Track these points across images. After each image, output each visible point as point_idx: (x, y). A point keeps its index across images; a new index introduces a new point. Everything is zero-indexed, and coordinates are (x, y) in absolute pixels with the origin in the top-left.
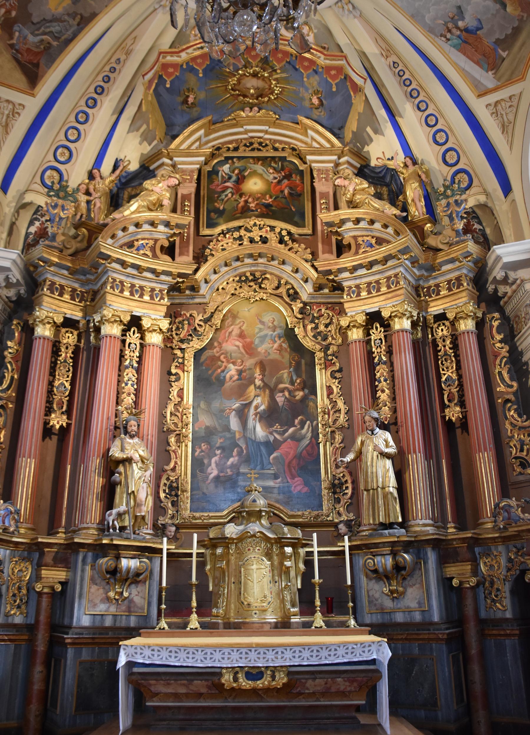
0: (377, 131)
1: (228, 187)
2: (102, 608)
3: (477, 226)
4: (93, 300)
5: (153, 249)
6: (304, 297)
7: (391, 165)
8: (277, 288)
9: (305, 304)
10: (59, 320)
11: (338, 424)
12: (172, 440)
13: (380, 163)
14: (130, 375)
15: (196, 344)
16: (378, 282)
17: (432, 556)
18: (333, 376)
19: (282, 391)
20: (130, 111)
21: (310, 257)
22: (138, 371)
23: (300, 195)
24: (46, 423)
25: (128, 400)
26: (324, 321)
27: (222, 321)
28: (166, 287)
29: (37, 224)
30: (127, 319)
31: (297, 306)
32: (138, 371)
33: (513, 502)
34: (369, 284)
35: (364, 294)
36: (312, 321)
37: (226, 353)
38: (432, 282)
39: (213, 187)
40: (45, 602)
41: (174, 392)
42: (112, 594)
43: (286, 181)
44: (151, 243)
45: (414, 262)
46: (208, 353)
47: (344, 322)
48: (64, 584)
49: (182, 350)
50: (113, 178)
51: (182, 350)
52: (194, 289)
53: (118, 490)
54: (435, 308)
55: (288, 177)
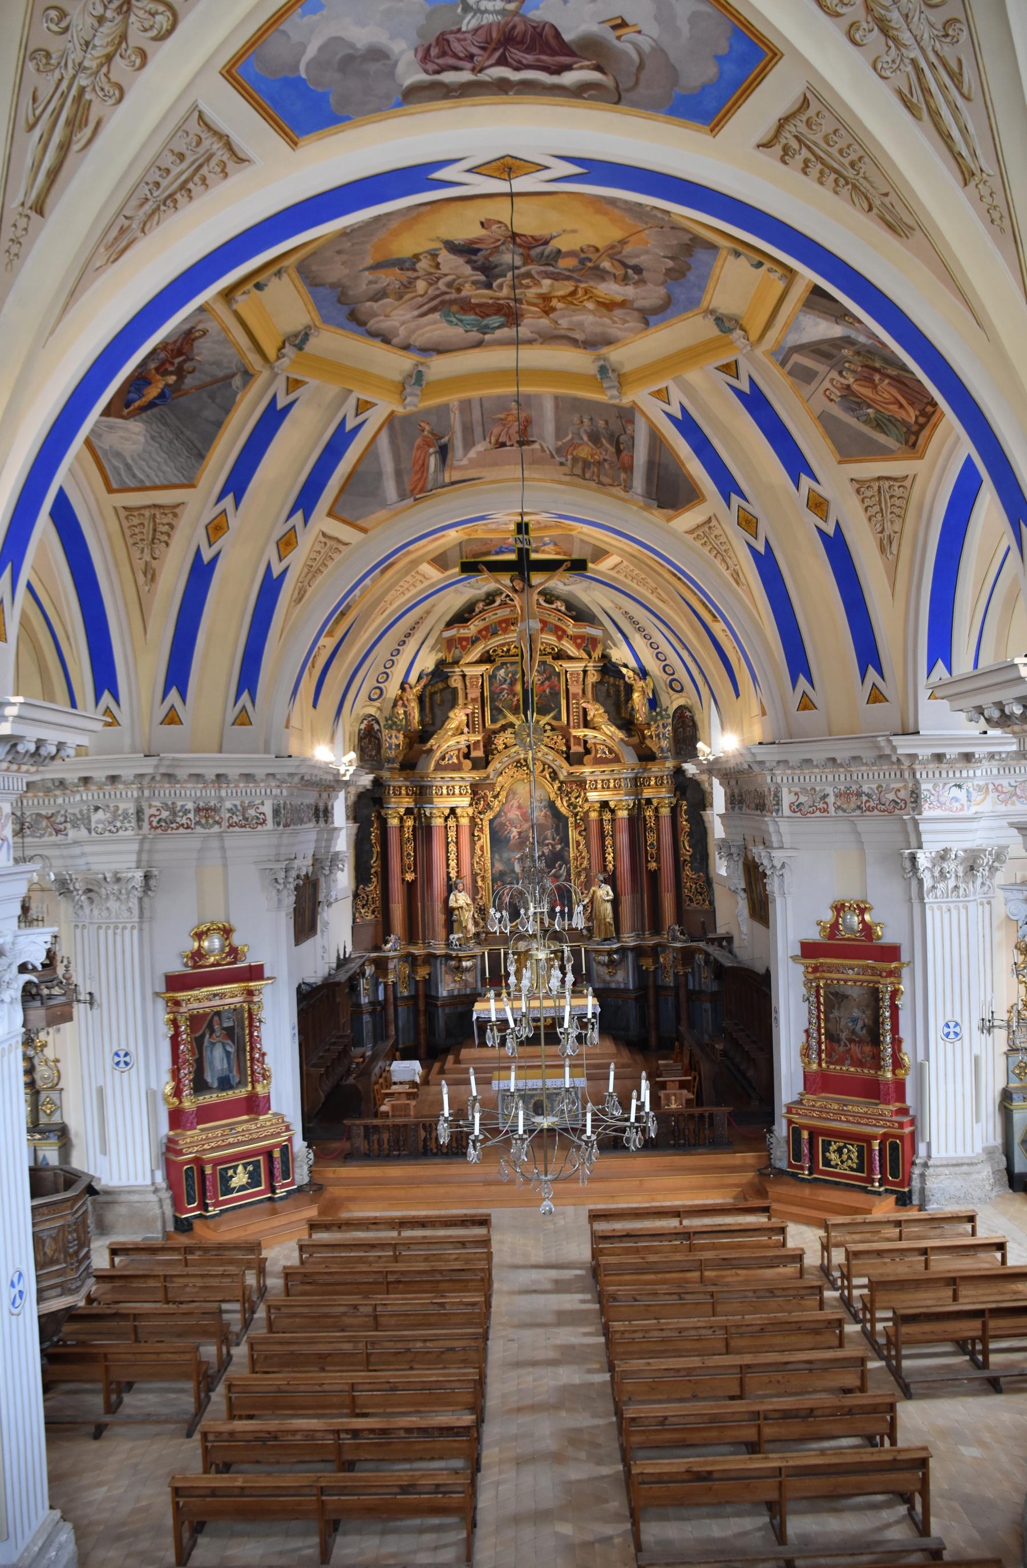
0: (615, 645)
1: (504, 689)
2: (452, 986)
3: (688, 713)
4: (421, 794)
5: (458, 757)
6: (562, 778)
7: (624, 670)
8: (543, 770)
9: (561, 782)
10: (402, 811)
11: (583, 866)
12: (479, 879)
13: (618, 662)
14: (452, 847)
15: (490, 815)
16: (608, 780)
17: (630, 956)
18: (580, 834)
19: (547, 845)
20: (430, 642)
21: (564, 749)
22: (457, 843)
23: (558, 694)
24: (403, 880)
25: (453, 863)
26: (575, 794)
27: (506, 798)
28: (468, 784)
29: (365, 722)
30: (447, 812)
31: (557, 785)
32: (457, 843)
33: (677, 928)
34: (603, 781)
35: (599, 786)
36: (567, 795)
37: (509, 820)
38: (646, 775)
39: (493, 689)
40: (421, 986)
41: (478, 847)
42: (457, 979)
43: (547, 683)
44: (456, 752)
45: (633, 769)
46: (498, 821)
47: (586, 806)
48: (429, 974)
49: (481, 820)
50: (419, 688)
51: (481, 820)
52: (488, 777)
53: (455, 925)
54: (647, 793)
55: (548, 678)
